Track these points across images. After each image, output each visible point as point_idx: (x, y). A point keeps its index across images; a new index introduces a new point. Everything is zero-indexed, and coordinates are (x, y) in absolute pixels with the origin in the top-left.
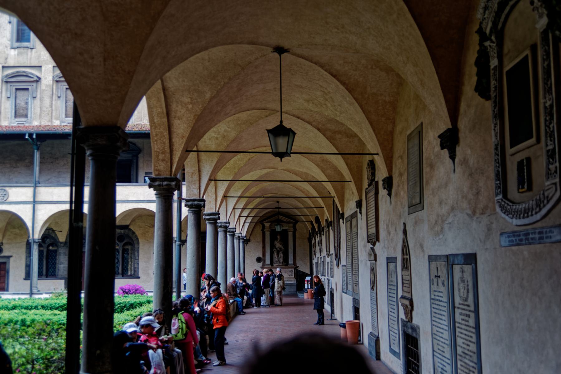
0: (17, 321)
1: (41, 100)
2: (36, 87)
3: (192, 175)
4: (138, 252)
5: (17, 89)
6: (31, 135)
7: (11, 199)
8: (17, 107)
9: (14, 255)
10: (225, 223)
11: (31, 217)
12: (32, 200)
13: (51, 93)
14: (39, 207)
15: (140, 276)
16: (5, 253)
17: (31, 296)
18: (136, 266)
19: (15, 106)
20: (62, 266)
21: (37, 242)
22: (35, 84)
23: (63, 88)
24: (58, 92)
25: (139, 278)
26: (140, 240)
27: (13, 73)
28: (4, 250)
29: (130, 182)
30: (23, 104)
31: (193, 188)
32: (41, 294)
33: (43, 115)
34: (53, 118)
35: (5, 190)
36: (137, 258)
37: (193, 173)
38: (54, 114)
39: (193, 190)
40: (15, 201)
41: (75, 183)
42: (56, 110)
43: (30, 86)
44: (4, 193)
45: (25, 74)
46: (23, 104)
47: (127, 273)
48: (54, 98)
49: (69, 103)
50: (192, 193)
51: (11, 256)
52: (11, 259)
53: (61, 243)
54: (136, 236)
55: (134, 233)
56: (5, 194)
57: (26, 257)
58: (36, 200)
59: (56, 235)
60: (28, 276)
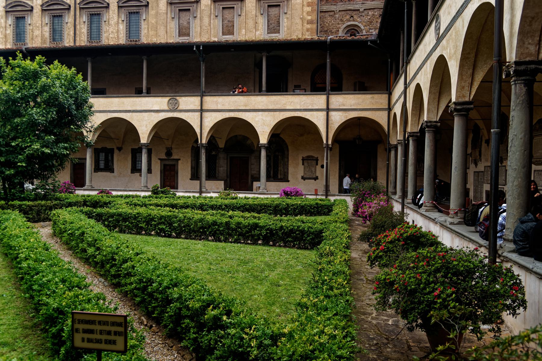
0: (221, 223)
1: (201, 19)
2: (197, 8)
3: (531, 22)
4: (288, 158)
5: (180, 10)
6: (198, 47)
7: (181, 107)
8: (181, 27)
9: (182, 159)
10: (435, 122)
11: (199, 124)
12: (199, 108)
13: (209, 12)
14: (205, 114)
15: (289, 179)
16: (175, 157)
17: (200, 194)
18: (286, 170)
19: (179, 26)
20: (221, 169)
21: (204, 147)
22: (195, 5)
23: (219, 8)
24: (215, 11)
25: (288, 181)
26: (289, 147)
28: (173, 154)
29: (287, 91)
30: (185, 24)
31: (529, 44)
32: (209, 193)
33: (203, 33)
34: (212, 36)
35: (176, 99)
36: (287, 163)
37: (533, 18)
38: (212, 33)
39: (529, 46)
40: (184, 109)
41: (407, 9)
42: (214, 28)
43: (191, 6)
46: (185, 24)
47: (278, 176)
48: (212, 17)
49: (225, 22)
50: (527, 51)
51: (179, 159)
52: (180, 162)
53: (221, 148)
54: (286, 144)
55: (284, 141)
56: (176, 103)
57: (191, 160)
58: (203, 108)
59: (216, 142)
60: (195, 176)
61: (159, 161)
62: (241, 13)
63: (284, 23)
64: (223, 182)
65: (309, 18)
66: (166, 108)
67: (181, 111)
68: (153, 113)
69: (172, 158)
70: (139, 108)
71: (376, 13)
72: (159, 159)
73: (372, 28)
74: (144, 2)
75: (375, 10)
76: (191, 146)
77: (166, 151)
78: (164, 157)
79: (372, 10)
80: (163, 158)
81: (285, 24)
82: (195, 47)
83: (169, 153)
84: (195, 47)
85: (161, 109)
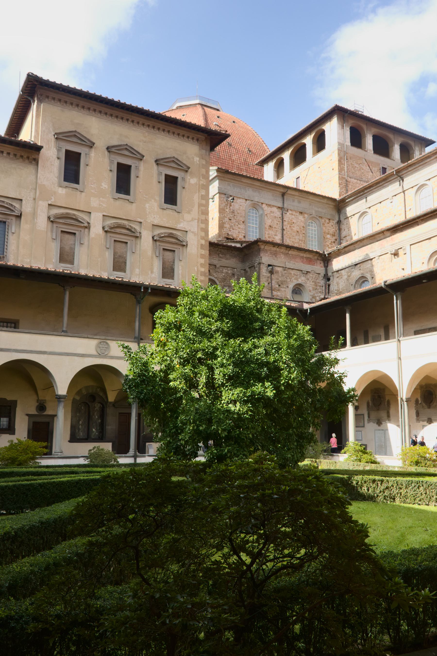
16: (49, 412)
27: (63, 214)
35: (107, 343)
43: (78, 231)
44: (106, 346)
45: (74, 217)
53: (111, 403)
57: (72, 417)
61: (27, 418)
62: (135, 251)
63: (179, 269)
64: (147, 444)
65: (203, 270)
66: (94, 353)
67: (112, 358)
68: (76, 358)
69: (45, 413)
70: (57, 350)
71: (230, 272)
72: (27, 415)
73: (226, 285)
74: (16, 212)
75: (229, 269)
76: (72, 399)
77: (37, 404)
78: (33, 411)
79: (226, 268)
80: (33, 413)
81: (180, 272)
82: (142, 288)
83: (41, 407)
84: (142, 288)
85: (88, 353)
